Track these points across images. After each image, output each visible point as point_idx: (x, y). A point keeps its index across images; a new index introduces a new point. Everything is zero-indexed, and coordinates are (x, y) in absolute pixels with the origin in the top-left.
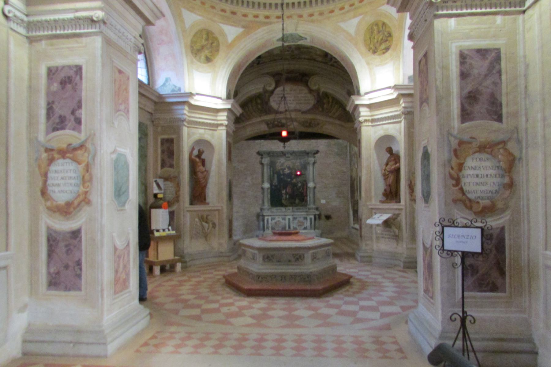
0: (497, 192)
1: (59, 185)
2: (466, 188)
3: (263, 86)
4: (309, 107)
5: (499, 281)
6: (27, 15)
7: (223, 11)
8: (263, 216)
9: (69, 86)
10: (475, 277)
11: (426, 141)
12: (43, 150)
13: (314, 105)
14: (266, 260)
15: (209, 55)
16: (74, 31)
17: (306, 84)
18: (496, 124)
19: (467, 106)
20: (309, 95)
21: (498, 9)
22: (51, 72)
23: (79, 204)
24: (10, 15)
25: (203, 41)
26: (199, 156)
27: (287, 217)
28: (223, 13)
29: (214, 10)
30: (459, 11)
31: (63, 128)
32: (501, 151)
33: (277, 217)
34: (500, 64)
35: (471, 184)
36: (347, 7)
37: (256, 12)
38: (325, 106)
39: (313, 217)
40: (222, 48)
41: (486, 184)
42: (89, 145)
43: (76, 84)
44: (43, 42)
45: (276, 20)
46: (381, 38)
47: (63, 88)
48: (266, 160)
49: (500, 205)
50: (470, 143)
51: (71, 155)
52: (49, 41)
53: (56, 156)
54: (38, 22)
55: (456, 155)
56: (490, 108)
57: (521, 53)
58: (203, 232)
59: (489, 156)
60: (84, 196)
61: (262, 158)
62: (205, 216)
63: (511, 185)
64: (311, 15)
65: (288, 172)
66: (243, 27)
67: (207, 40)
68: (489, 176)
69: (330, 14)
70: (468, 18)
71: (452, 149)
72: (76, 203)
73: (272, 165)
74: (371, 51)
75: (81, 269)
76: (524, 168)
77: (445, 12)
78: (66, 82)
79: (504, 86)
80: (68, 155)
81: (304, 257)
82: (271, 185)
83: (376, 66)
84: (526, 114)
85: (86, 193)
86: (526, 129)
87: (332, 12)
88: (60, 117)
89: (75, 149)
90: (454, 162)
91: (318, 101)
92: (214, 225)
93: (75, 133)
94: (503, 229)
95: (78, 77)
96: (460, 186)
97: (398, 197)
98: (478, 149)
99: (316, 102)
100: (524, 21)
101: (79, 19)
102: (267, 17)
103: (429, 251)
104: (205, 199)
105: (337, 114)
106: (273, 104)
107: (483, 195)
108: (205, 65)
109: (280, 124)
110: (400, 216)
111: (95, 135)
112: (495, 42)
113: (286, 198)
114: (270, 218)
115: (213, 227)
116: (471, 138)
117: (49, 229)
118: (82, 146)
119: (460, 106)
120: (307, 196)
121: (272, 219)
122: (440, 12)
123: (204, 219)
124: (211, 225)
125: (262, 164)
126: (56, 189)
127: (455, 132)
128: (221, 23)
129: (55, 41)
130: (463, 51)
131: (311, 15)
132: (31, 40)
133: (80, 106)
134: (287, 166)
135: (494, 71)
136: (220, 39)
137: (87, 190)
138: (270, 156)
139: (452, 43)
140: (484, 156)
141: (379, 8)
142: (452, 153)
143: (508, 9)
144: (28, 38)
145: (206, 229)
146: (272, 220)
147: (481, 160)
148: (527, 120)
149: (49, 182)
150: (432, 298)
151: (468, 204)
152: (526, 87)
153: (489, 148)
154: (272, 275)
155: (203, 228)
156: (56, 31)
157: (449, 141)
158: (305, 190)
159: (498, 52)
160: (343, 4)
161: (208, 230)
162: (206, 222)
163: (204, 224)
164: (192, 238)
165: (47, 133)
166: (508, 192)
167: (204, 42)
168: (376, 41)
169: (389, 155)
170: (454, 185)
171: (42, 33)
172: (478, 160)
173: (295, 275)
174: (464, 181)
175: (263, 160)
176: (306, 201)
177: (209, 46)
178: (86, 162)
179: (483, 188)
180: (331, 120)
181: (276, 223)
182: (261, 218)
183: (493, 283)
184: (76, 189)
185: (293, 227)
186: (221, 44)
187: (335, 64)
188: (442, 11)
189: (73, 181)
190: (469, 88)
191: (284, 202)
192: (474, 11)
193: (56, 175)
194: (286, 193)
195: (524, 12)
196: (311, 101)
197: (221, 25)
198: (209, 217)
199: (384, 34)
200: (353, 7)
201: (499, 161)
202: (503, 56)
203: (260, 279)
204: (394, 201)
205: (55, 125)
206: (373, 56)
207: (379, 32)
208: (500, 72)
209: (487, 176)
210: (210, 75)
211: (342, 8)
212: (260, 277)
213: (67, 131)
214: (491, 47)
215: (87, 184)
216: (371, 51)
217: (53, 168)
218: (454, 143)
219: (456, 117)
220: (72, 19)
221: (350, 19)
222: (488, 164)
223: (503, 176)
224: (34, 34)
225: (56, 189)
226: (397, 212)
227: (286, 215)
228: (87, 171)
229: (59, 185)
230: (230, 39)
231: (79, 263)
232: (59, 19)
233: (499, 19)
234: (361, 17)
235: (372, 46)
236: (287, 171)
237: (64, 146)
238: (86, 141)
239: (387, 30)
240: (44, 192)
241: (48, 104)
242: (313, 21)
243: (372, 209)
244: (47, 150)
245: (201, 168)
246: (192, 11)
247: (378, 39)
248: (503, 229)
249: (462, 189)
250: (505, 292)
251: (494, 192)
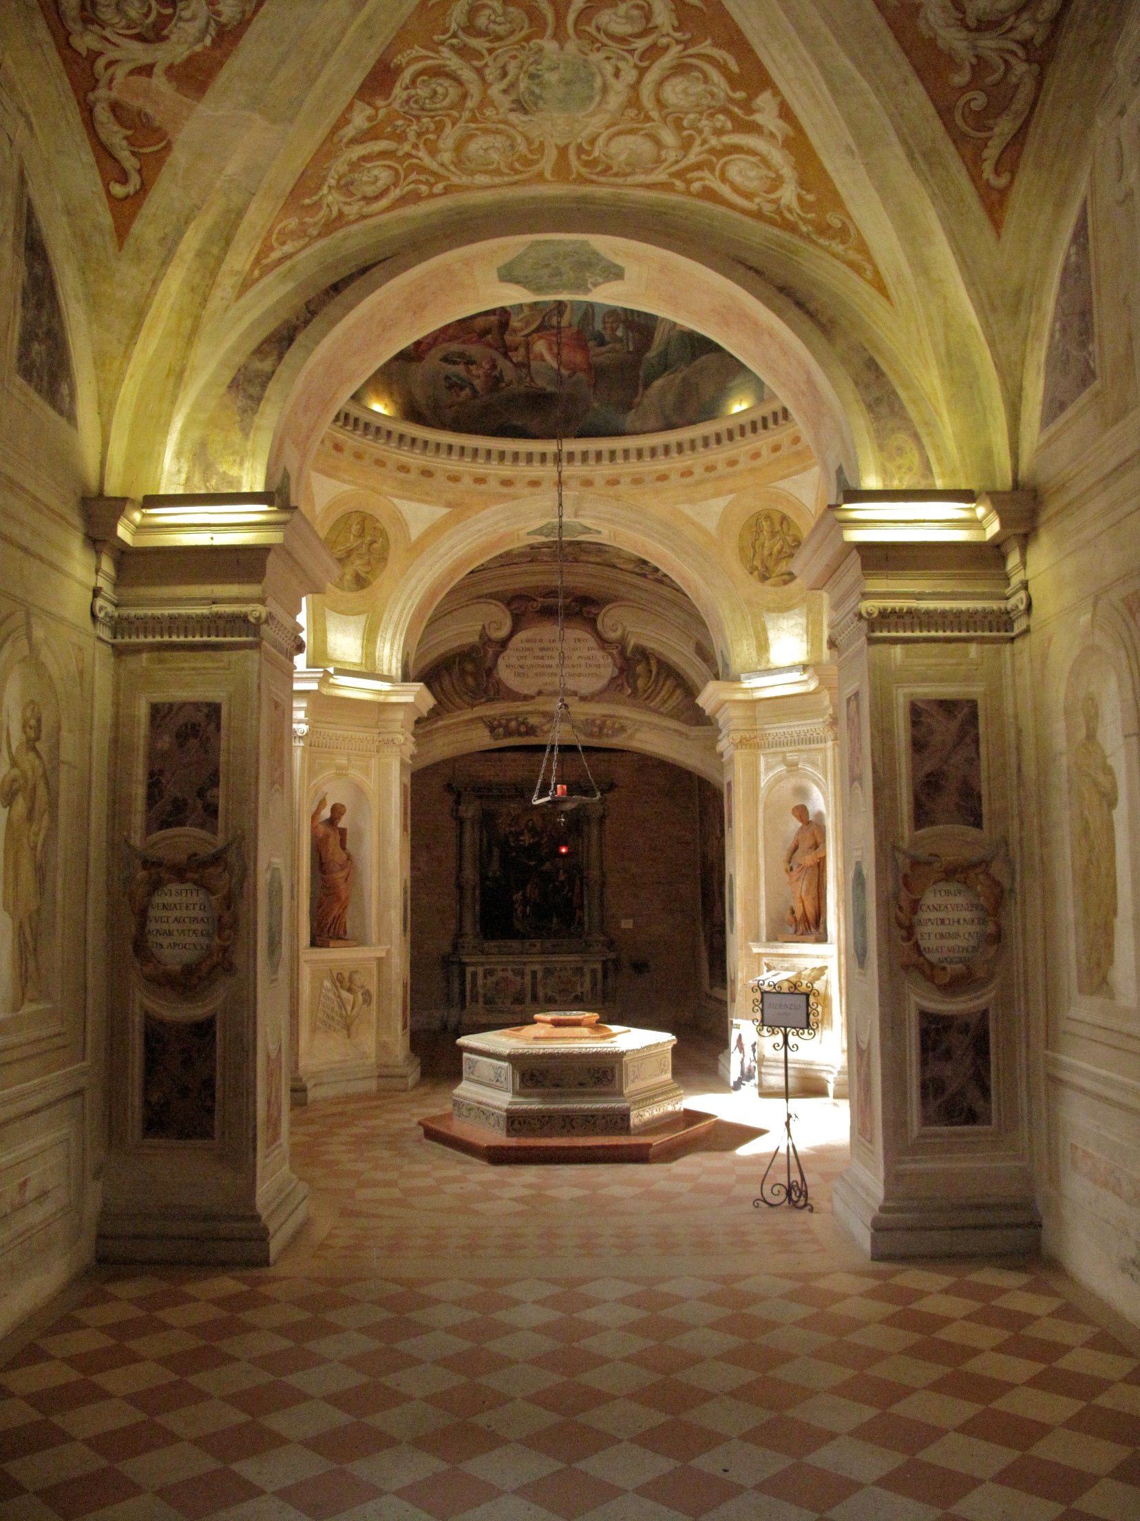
0: (975, 949)
1: (170, 933)
2: (923, 944)
3: (480, 628)
4: (599, 684)
5: (979, 1106)
6: (116, 606)
7: (404, 468)
8: (463, 965)
9: (193, 742)
10: (939, 1101)
11: (859, 853)
12: (138, 862)
13: (613, 680)
14: (529, 1083)
15: (362, 571)
16: (205, 639)
17: (591, 622)
18: (973, 831)
19: (923, 798)
20: (599, 654)
21: (972, 634)
22: (158, 713)
23: (209, 973)
24: (101, 615)
25: (352, 537)
26: (332, 822)
27: (528, 969)
28: (402, 475)
29: (382, 470)
30: (909, 634)
32: (981, 877)
33: (499, 967)
34: (976, 726)
35: (932, 937)
36: (699, 472)
37: (480, 468)
38: (641, 683)
39: (598, 966)
40: (396, 555)
41: (956, 935)
42: (232, 858)
43: (208, 739)
44: (145, 656)
45: (527, 490)
46: (778, 547)
47: (181, 746)
48: (470, 811)
49: (981, 973)
50: (929, 864)
51: (196, 876)
52: (155, 654)
53: (165, 876)
54: (138, 618)
55: (906, 884)
56: (962, 803)
57: (1010, 711)
58: (341, 1016)
59: (960, 887)
60: (221, 955)
61: (458, 803)
62: (346, 975)
63: (997, 938)
64: (614, 482)
65: (531, 841)
66: (448, 505)
67: (361, 534)
68: (962, 921)
69: (659, 484)
70: (922, 646)
71: (901, 875)
72: (205, 968)
73: (487, 820)
74: (756, 573)
75: (213, 1096)
76: (1018, 908)
77: (885, 634)
79: (984, 764)
80: (189, 875)
81: (613, 1076)
82: (484, 878)
83: (769, 610)
84: (1020, 814)
85: (225, 950)
86: (1021, 839)
87: (663, 478)
88: (175, 800)
89: (204, 864)
90: (904, 894)
91: (622, 670)
92: (367, 994)
94: (985, 1013)
95: (212, 727)
96: (914, 940)
97: (822, 926)
98: (943, 875)
99: (617, 671)
100: (1013, 655)
101: (219, 616)
102: (506, 483)
103: (866, 1055)
104: (345, 932)
105: (671, 703)
106: (505, 673)
107: (951, 955)
108: (350, 595)
109: (523, 729)
110: (826, 971)
111: (243, 838)
112: (968, 689)
113: (524, 912)
114: (480, 970)
115: (365, 1001)
116: (931, 855)
117: (148, 1017)
118: (217, 859)
119: (911, 799)
120: (581, 907)
121: (489, 973)
122: (878, 634)
123: (343, 981)
124: (360, 998)
125: (461, 822)
126: (166, 941)
127: (905, 845)
128: (397, 496)
129: (167, 655)
130: (919, 704)
131: (614, 482)
132: (120, 652)
133: (215, 783)
134: (526, 825)
135: (968, 739)
136: (392, 533)
137: (228, 943)
138: (480, 797)
139: (898, 687)
140: (953, 886)
141: (774, 484)
142: (901, 882)
143: (987, 634)
144: (113, 646)
145: (349, 1009)
146: (485, 977)
147: (948, 893)
148: (1022, 823)
149: (152, 926)
150: (870, 1142)
151: (928, 972)
152: (1019, 769)
153: (962, 872)
154: (543, 1117)
155: (342, 1004)
156: (170, 637)
157: (895, 859)
158: (577, 889)
159: (973, 705)
160: (689, 462)
161: (353, 1008)
162: (350, 990)
163: (345, 994)
164: (314, 1030)
165: (149, 831)
166: (992, 951)
167: (353, 542)
168: (766, 553)
169: (800, 824)
170: (903, 939)
171: (142, 639)
172: (943, 893)
173: (593, 1116)
174: (921, 930)
175: (462, 808)
176: (581, 923)
177: (364, 549)
178: (225, 892)
179: (951, 943)
180: (655, 719)
181: (497, 984)
182: (455, 969)
183: (970, 1109)
184: (204, 941)
185: (546, 994)
186: (392, 547)
187: (664, 579)
188: (881, 631)
189: (199, 927)
190: (928, 768)
191: (518, 925)
192: (933, 634)
193: (165, 913)
194: (526, 901)
195: (1012, 640)
196: (607, 669)
197: (396, 501)
198: (356, 977)
199: (784, 540)
200: (712, 474)
201: (978, 896)
202: (981, 713)
203: (516, 1126)
204: (812, 937)
205: (164, 817)
206: (759, 585)
207: (773, 534)
208: (976, 741)
209: (959, 921)
210: (363, 618)
211: (687, 473)
212: (515, 1121)
214: (961, 697)
215: (227, 932)
216: (756, 573)
217: (158, 899)
218: (904, 863)
219: (906, 818)
220: (204, 617)
221: (706, 498)
222: (960, 900)
223: (983, 922)
224: (127, 640)
226: (819, 963)
227: (525, 964)
228: (229, 907)
229: (170, 933)
230: (415, 532)
231: (209, 1084)
232: (180, 615)
233: (973, 649)
234: (731, 496)
235: (757, 563)
236: (527, 839)
237: (183, 857)
238: (225, 850)
239: (791, 532)
240: (140, 947)
241: (151, 774)
242: (618, 498)
243: (759, 954)
244: (147, 864)
245: (336, 855)
246: (329, 476)
247: (772, 548)
248: (985, 1013)
249: (917, 946)
250: (990, 1123)
251: (970, 949)
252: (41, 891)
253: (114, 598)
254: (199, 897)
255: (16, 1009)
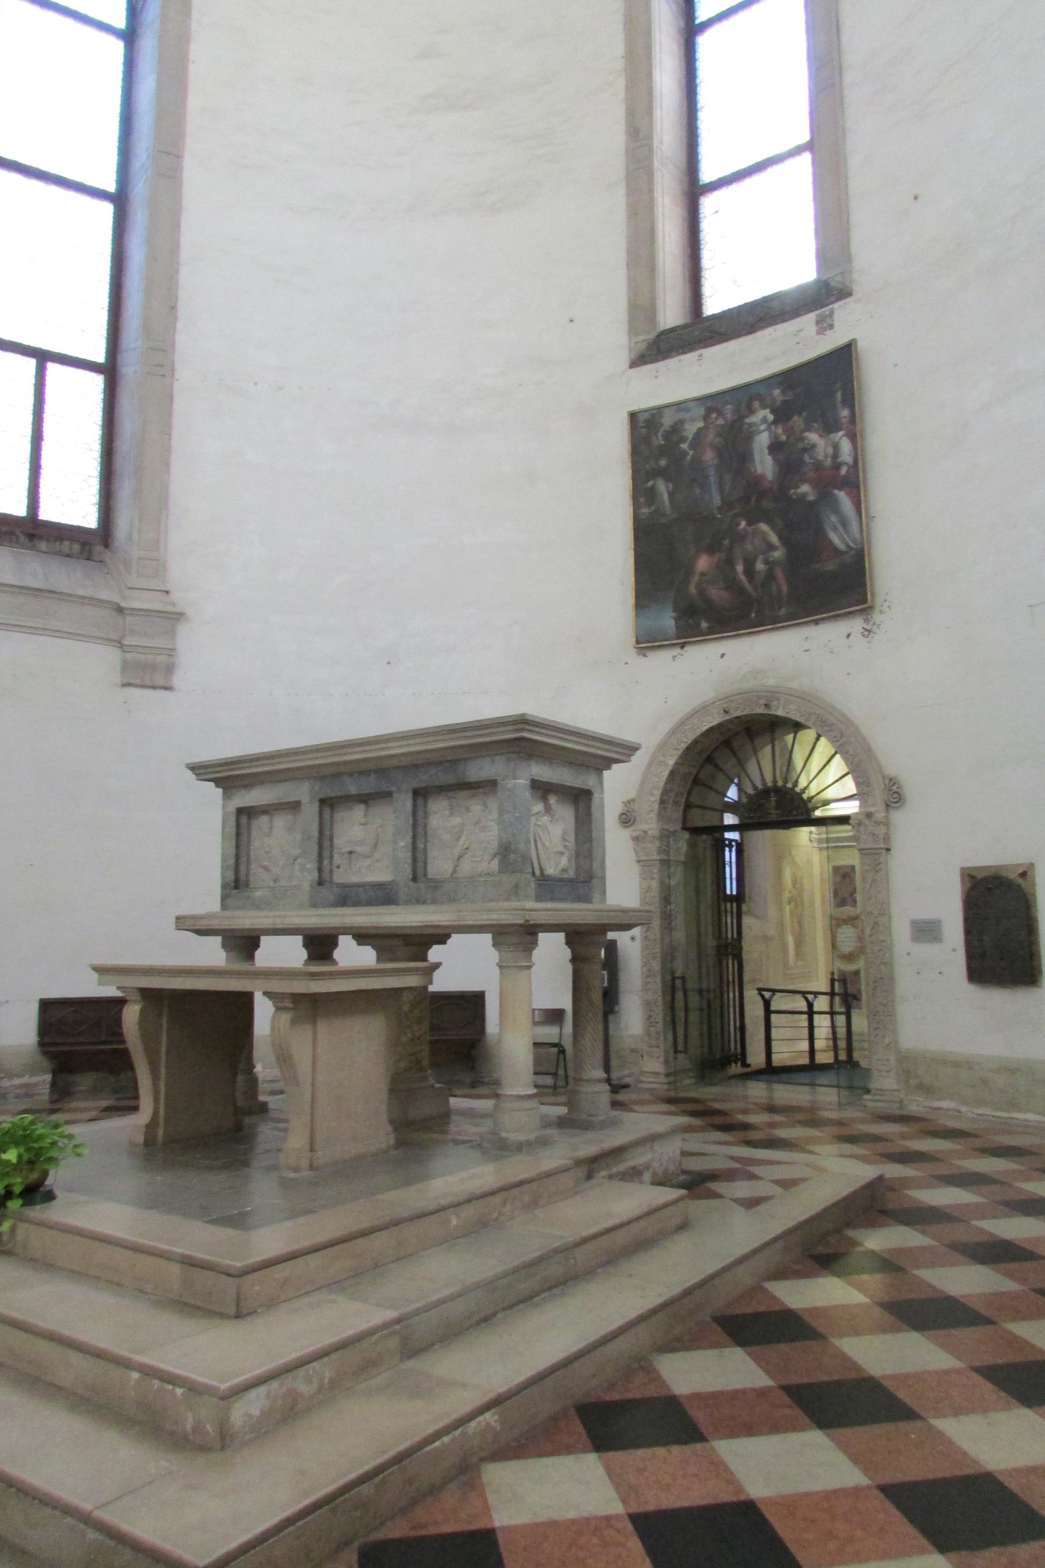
6: (818, 834)
31: (844, 906)
78: (845, 876)
93: (853, 909)
144: (818, 848)
184: (855, 944)
213: (847, 907)
225: (841, 943)
237: (845, 917)
252: (800, 927)
253: (817, 833)
254: (852, 930)
255: (795, 963)
